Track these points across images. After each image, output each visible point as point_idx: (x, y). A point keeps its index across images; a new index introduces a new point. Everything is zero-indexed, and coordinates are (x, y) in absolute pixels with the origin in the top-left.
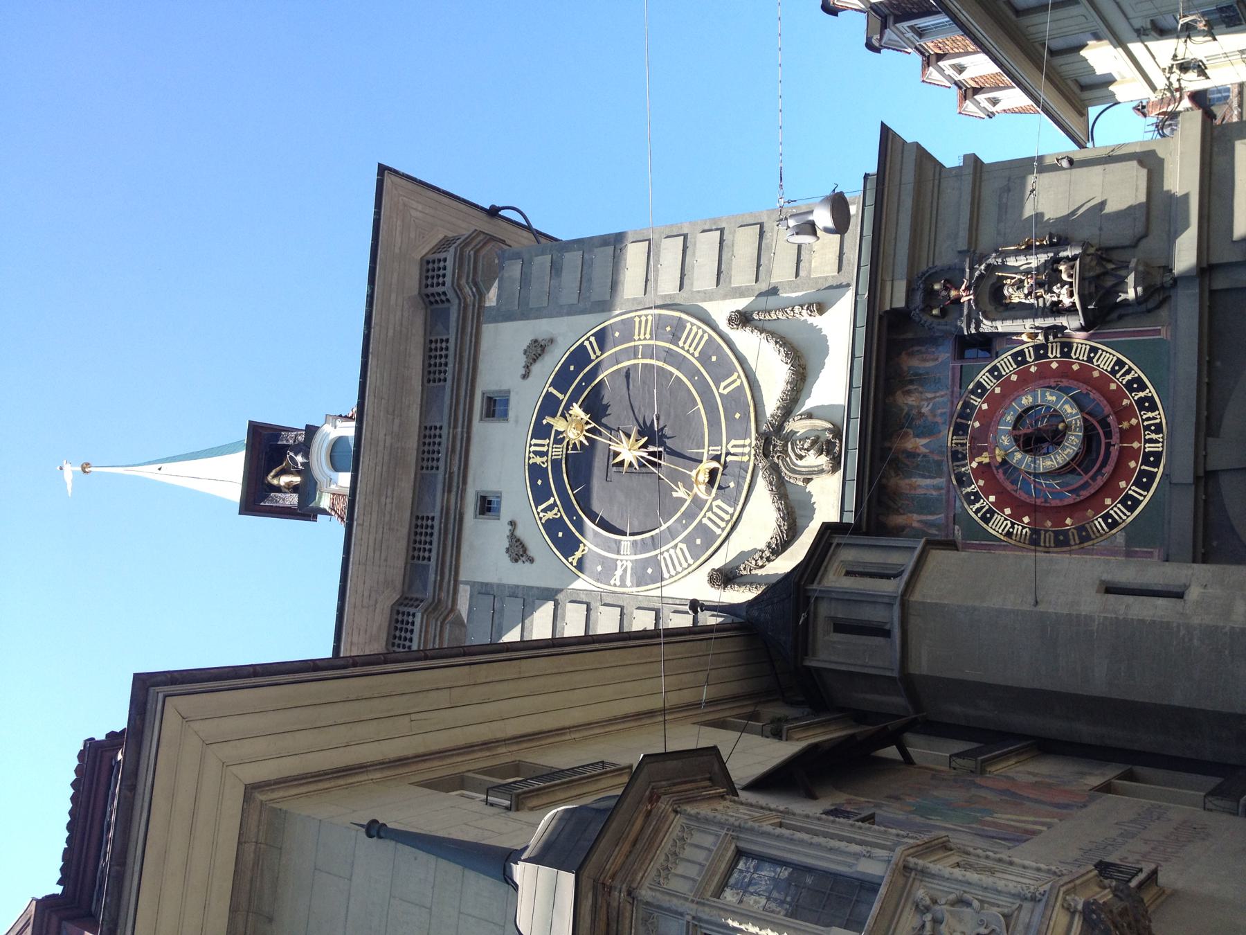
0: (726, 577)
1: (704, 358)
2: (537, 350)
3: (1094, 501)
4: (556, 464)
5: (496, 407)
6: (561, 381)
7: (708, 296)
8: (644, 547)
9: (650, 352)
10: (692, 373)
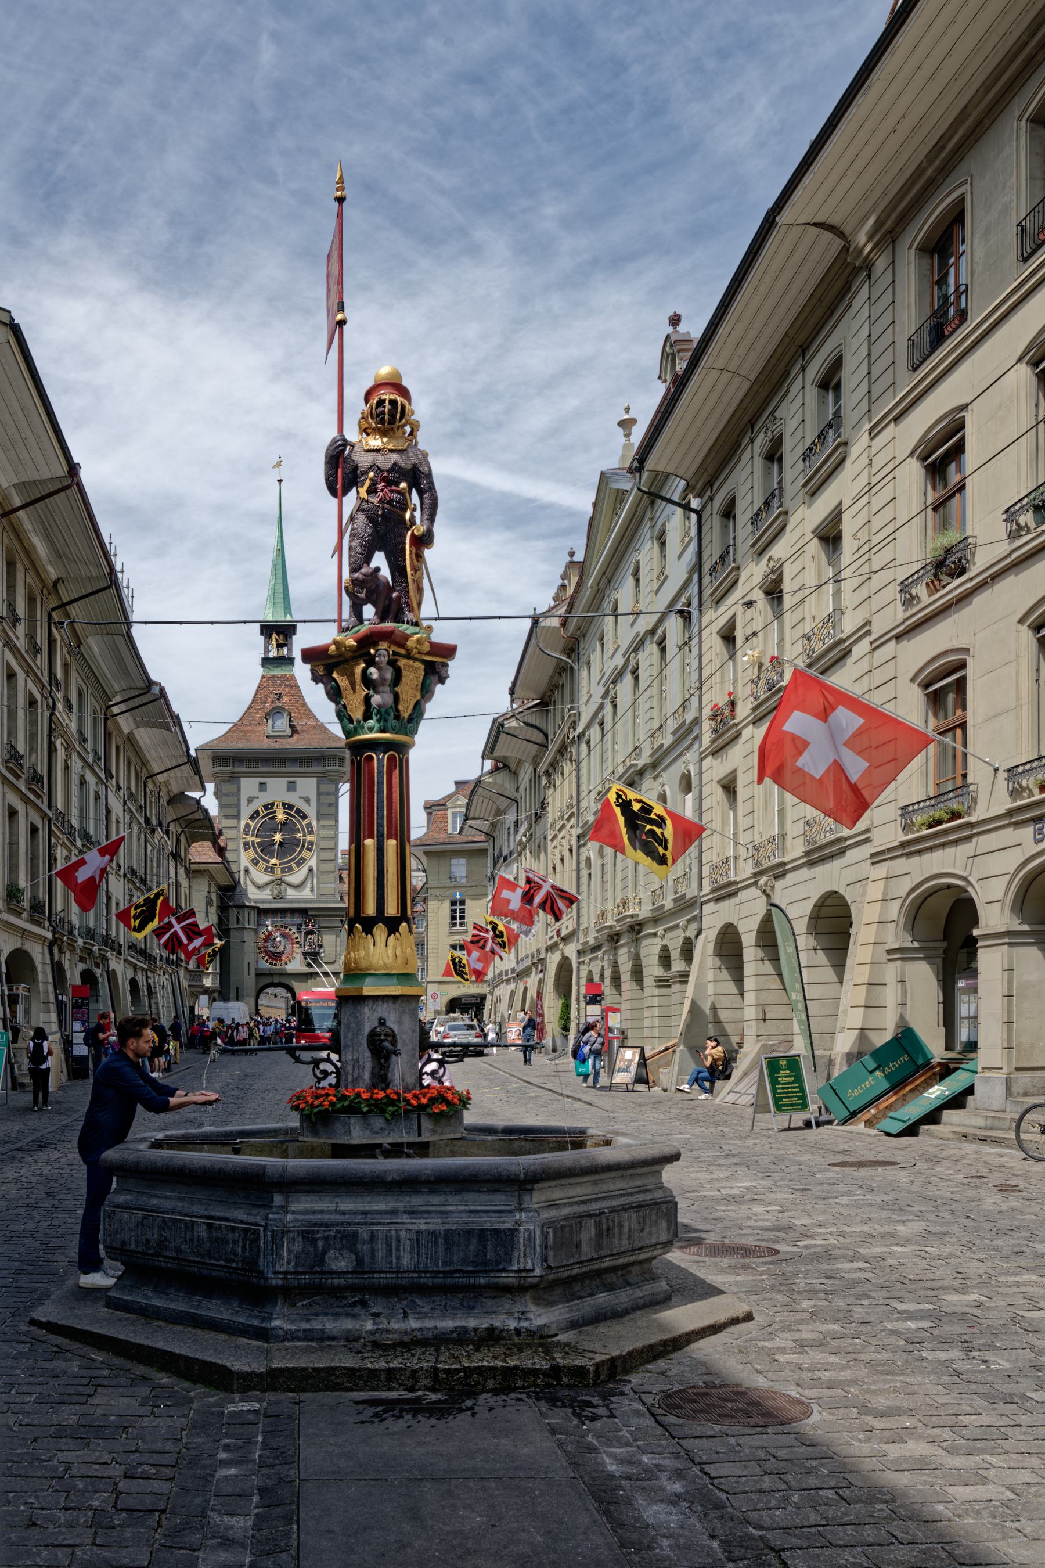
0: (247, 871)
1: (302, 858)
2: (307, 800)
3: (267, 954)
4: (274, 812)
5: (291, 787)
6: (298, 811)
7: (318, 857)
8: (253, 844)
9: (304, 840)
10: (298, 855)
